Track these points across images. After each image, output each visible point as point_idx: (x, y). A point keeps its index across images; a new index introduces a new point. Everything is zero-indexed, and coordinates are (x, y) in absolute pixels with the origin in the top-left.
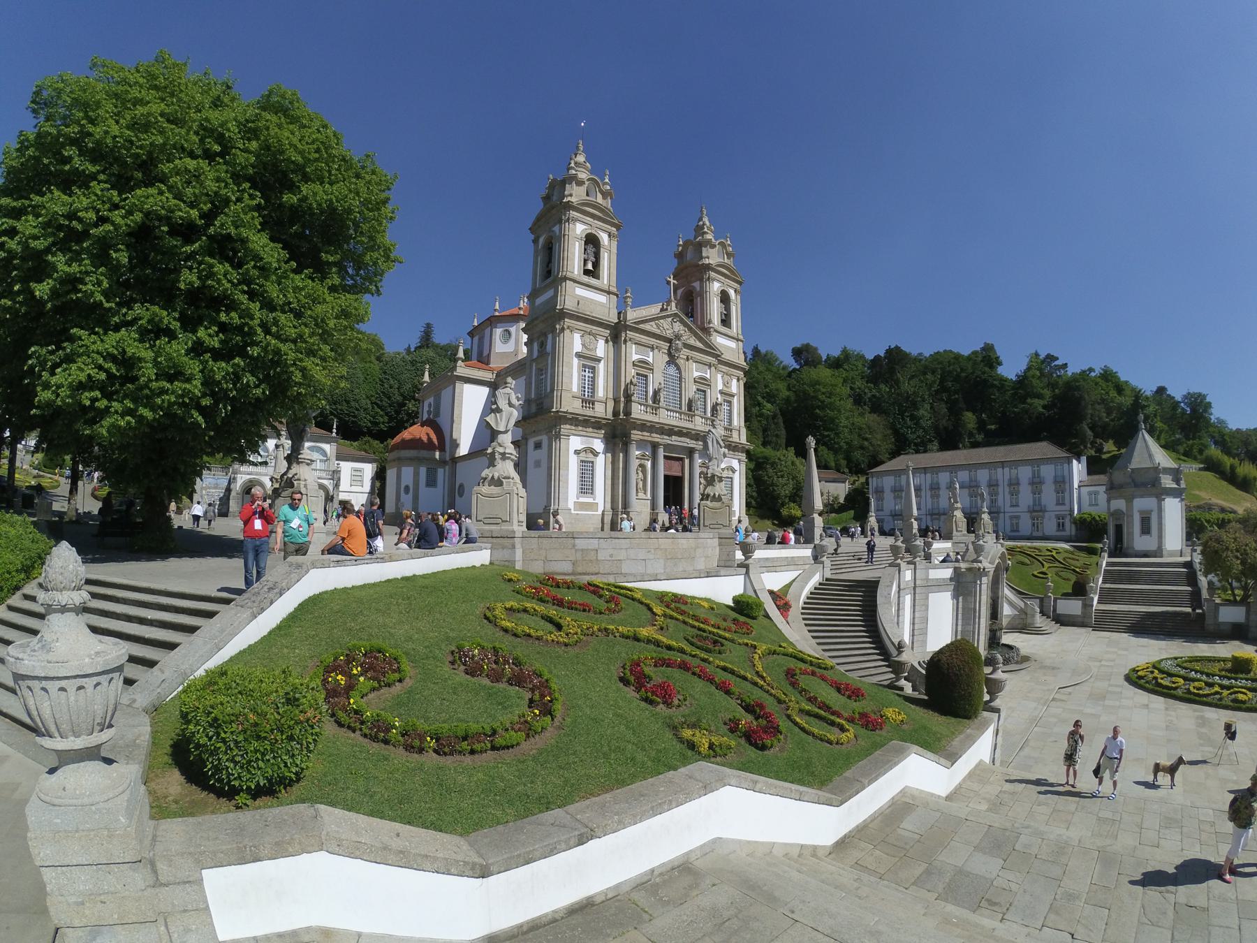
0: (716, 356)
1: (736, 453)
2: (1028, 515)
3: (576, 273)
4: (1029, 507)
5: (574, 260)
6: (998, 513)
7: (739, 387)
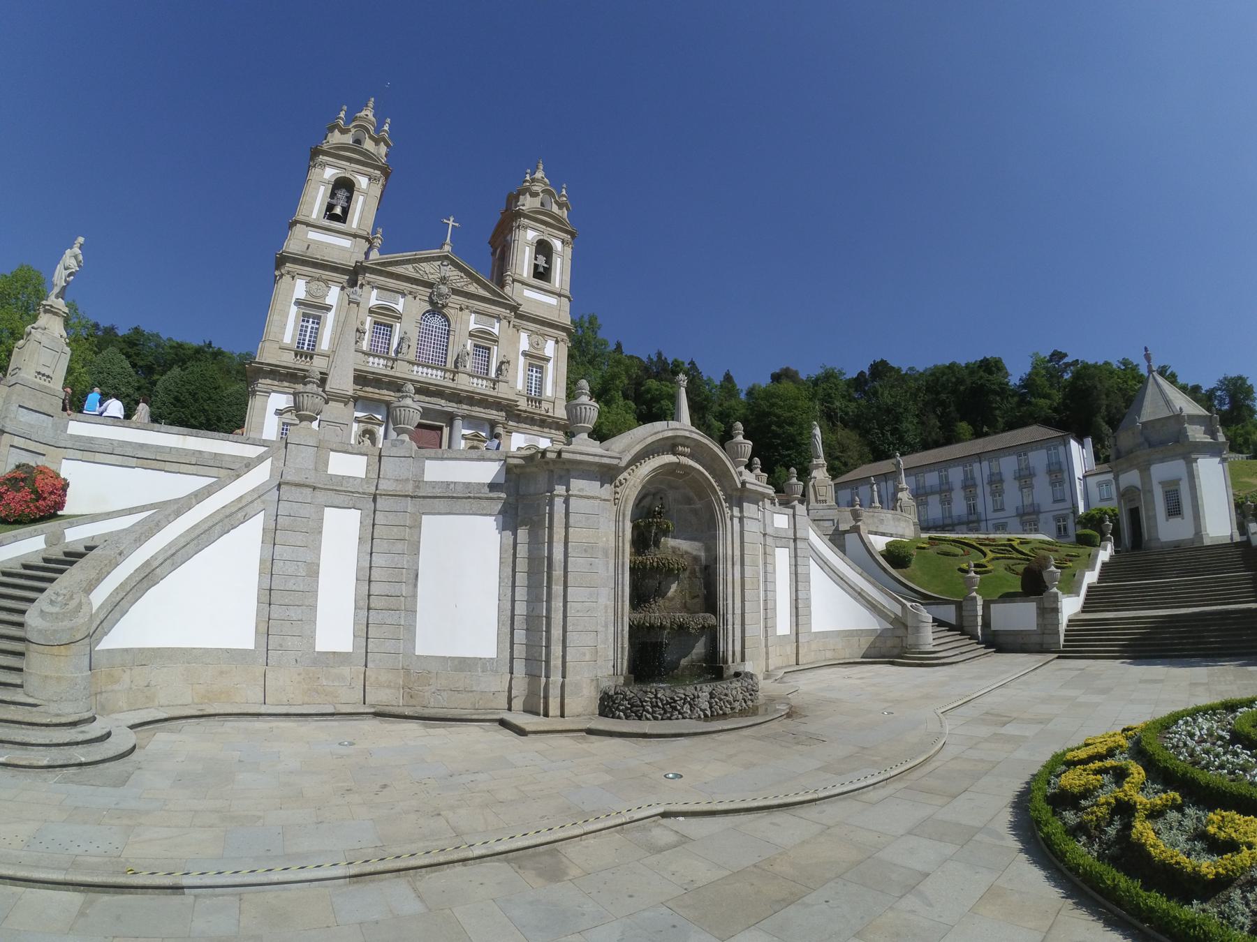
0: (514, 309)
1: (546, 430)
2: (1018, 519)
3: (314, 216)
4: (1017, 508)
5: (313, 204)
6: (979, 521)
7: (557, 350)
